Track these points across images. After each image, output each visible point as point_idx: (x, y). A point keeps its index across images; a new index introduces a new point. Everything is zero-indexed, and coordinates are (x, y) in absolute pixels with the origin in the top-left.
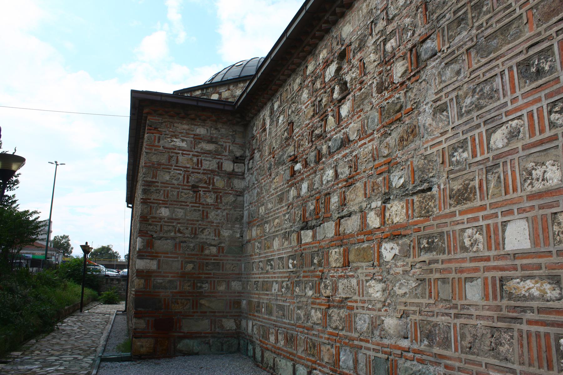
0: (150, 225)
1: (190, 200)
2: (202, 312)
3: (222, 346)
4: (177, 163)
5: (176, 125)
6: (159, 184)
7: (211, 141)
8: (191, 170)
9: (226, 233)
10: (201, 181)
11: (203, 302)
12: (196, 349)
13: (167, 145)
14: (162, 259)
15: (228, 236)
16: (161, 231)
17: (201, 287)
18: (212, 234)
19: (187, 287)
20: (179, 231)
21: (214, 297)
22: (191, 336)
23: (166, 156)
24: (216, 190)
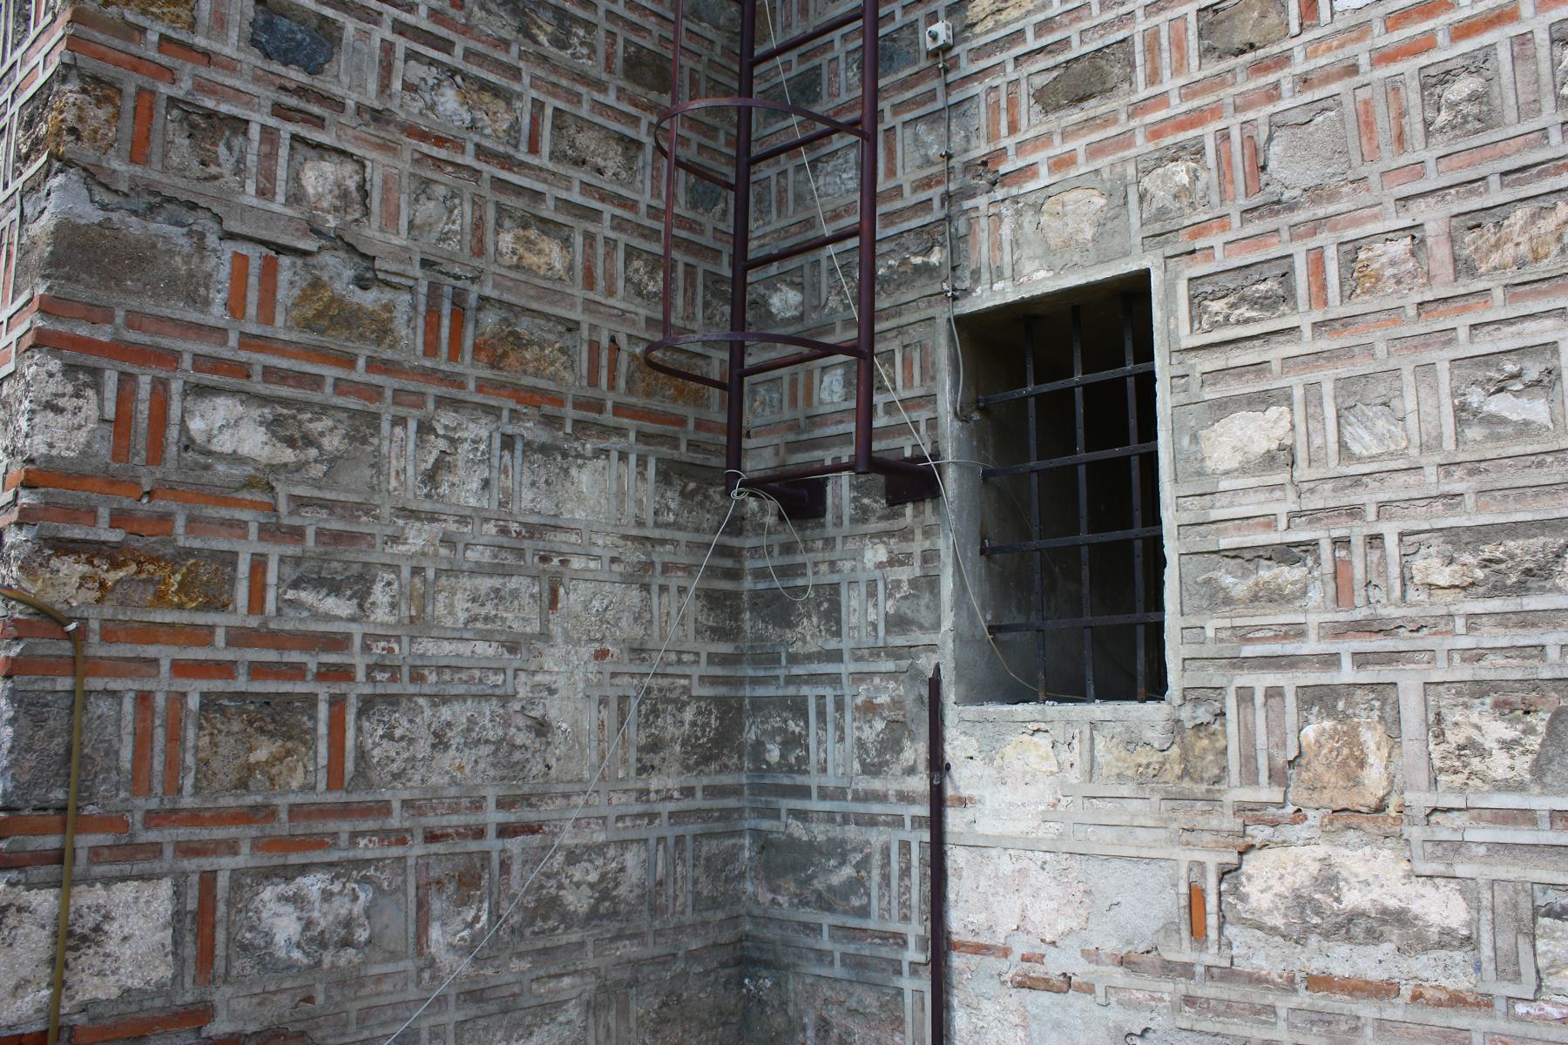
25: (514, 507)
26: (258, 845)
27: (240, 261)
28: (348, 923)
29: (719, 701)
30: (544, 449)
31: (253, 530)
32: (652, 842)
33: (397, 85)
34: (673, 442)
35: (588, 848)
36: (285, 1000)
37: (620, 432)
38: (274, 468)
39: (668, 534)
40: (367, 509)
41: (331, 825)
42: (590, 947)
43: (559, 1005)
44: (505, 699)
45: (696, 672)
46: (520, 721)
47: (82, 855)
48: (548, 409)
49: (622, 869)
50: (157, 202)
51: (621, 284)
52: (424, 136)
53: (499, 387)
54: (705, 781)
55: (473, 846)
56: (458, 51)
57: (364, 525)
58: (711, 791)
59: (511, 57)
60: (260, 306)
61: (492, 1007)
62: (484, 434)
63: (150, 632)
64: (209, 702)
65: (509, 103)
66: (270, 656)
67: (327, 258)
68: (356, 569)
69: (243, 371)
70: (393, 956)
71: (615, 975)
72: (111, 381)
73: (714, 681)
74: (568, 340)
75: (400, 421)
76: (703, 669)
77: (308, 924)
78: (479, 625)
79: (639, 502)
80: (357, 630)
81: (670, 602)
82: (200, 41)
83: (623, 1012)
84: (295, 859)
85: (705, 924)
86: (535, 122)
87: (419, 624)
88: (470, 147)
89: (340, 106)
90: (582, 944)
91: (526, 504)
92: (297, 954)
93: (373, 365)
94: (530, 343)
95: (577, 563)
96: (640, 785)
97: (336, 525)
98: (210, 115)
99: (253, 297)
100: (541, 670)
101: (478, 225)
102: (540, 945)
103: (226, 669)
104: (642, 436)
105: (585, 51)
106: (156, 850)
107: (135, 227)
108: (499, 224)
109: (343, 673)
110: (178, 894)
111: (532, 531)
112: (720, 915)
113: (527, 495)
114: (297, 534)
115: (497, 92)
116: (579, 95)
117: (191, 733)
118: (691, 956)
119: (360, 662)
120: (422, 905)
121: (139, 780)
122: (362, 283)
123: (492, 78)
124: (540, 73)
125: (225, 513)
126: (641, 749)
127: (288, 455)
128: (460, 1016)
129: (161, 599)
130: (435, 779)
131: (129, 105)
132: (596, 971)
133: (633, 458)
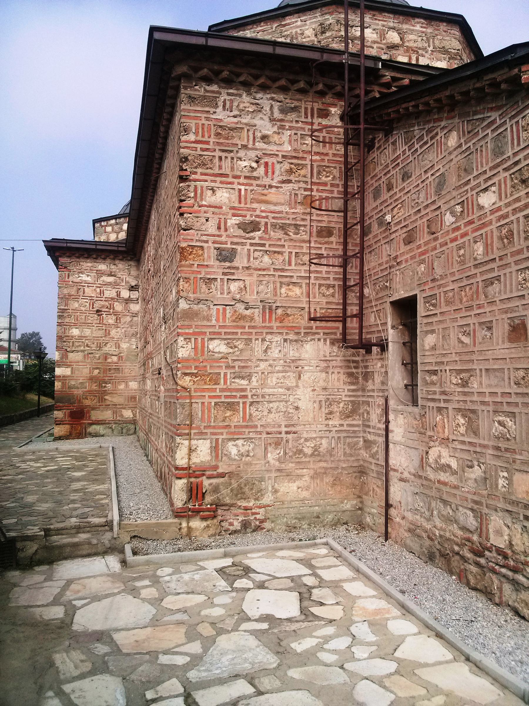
0: (65, 342)
1: (95, 322)
2: (106, 405)
3: (122, 429)
4: (84, 293)
5: (81, 263)
6: (70, 311)
7: (110, 275)
9: (124, 346)
10: (103, 306)
11: (106, 397)
12: (102, 432)
13: (75, 280)
14: (75, 366)
15: (127, 348)
16: (73, 346)
17: (105, 387)
18: (114, 347)
19: (94, 387)
20: (87, 346)
22: (98, 423)
23: (75, 288)
24: (116, 314)
25: (288, 356)
27: (218, 310)
28: (248, 451)
29: (352, 402)
30: (296, 341)
31: (224, 367)
32: (330, 438)
33: (252, 259)
34: (335, 334)
35: (311, 438)
36: (234, 467)
37: (318, 333)
40: (250, 360)
41: (244, 430)
42: (312, 463)
43: (303, 476)
44: (286, 402)
45: (344, 394)
46: (291, 407)
47: (192, 434)
48: (296, 331)
50: (199, 301)
52: (260, 270)
53: (283, 327)
54: (347, 423)
55: (279, 436)
56: (267, 246)
57: (250, 364)
58: (349, 425)
59: (282, 243)
61: (284, 474)
62: (279, 339)
63: (203, 390)
64: (216, 404)
65: (282, 254)
66: (229, 394)
67: (237, 305)
68: (248, 374)
69: (220, 333)
70: (259, 459)
71: (319, 471)
72: (193, 340)
73: (350, 396)
74: (302, 312)
75: (257, 339)
76: (346, 393)
77: (239, 451)
78: (280, 385)
79: (325, 351)
80: (248, 387)
82: (206, 263)
83: (322, 480)
85: (348, 460)
86: (290, 258)
87: (263, 385)
88: (272, 269)
89: (237, 268)
90: (309, 462)
92: (236, 457)
93: (249, 327)
94: (291, 315)
95: (306, 368)
96: (326, 423)
97: (242, 365)
98: (209, 279)
99: (221, 318)
101: (275, 289)
103: (219, 397)
104: (324, 333)
105: (304, 233)
107: (195, 307)
108: (281, 287)
109: (246, 397)
111: (293, 361)
112: (353, 459)
113: (291, 352)
114: (234, 367)
115: (279, 253)
117: (213, 410)
119: (250, 395)
120: (266, 449)
121: (202, 420)
122: (246, 309)
124: (291, 244)
127: (231, 350)
129: (205, 383)
130: (269, 420)
132: (313, 469)
133: (322, 340)
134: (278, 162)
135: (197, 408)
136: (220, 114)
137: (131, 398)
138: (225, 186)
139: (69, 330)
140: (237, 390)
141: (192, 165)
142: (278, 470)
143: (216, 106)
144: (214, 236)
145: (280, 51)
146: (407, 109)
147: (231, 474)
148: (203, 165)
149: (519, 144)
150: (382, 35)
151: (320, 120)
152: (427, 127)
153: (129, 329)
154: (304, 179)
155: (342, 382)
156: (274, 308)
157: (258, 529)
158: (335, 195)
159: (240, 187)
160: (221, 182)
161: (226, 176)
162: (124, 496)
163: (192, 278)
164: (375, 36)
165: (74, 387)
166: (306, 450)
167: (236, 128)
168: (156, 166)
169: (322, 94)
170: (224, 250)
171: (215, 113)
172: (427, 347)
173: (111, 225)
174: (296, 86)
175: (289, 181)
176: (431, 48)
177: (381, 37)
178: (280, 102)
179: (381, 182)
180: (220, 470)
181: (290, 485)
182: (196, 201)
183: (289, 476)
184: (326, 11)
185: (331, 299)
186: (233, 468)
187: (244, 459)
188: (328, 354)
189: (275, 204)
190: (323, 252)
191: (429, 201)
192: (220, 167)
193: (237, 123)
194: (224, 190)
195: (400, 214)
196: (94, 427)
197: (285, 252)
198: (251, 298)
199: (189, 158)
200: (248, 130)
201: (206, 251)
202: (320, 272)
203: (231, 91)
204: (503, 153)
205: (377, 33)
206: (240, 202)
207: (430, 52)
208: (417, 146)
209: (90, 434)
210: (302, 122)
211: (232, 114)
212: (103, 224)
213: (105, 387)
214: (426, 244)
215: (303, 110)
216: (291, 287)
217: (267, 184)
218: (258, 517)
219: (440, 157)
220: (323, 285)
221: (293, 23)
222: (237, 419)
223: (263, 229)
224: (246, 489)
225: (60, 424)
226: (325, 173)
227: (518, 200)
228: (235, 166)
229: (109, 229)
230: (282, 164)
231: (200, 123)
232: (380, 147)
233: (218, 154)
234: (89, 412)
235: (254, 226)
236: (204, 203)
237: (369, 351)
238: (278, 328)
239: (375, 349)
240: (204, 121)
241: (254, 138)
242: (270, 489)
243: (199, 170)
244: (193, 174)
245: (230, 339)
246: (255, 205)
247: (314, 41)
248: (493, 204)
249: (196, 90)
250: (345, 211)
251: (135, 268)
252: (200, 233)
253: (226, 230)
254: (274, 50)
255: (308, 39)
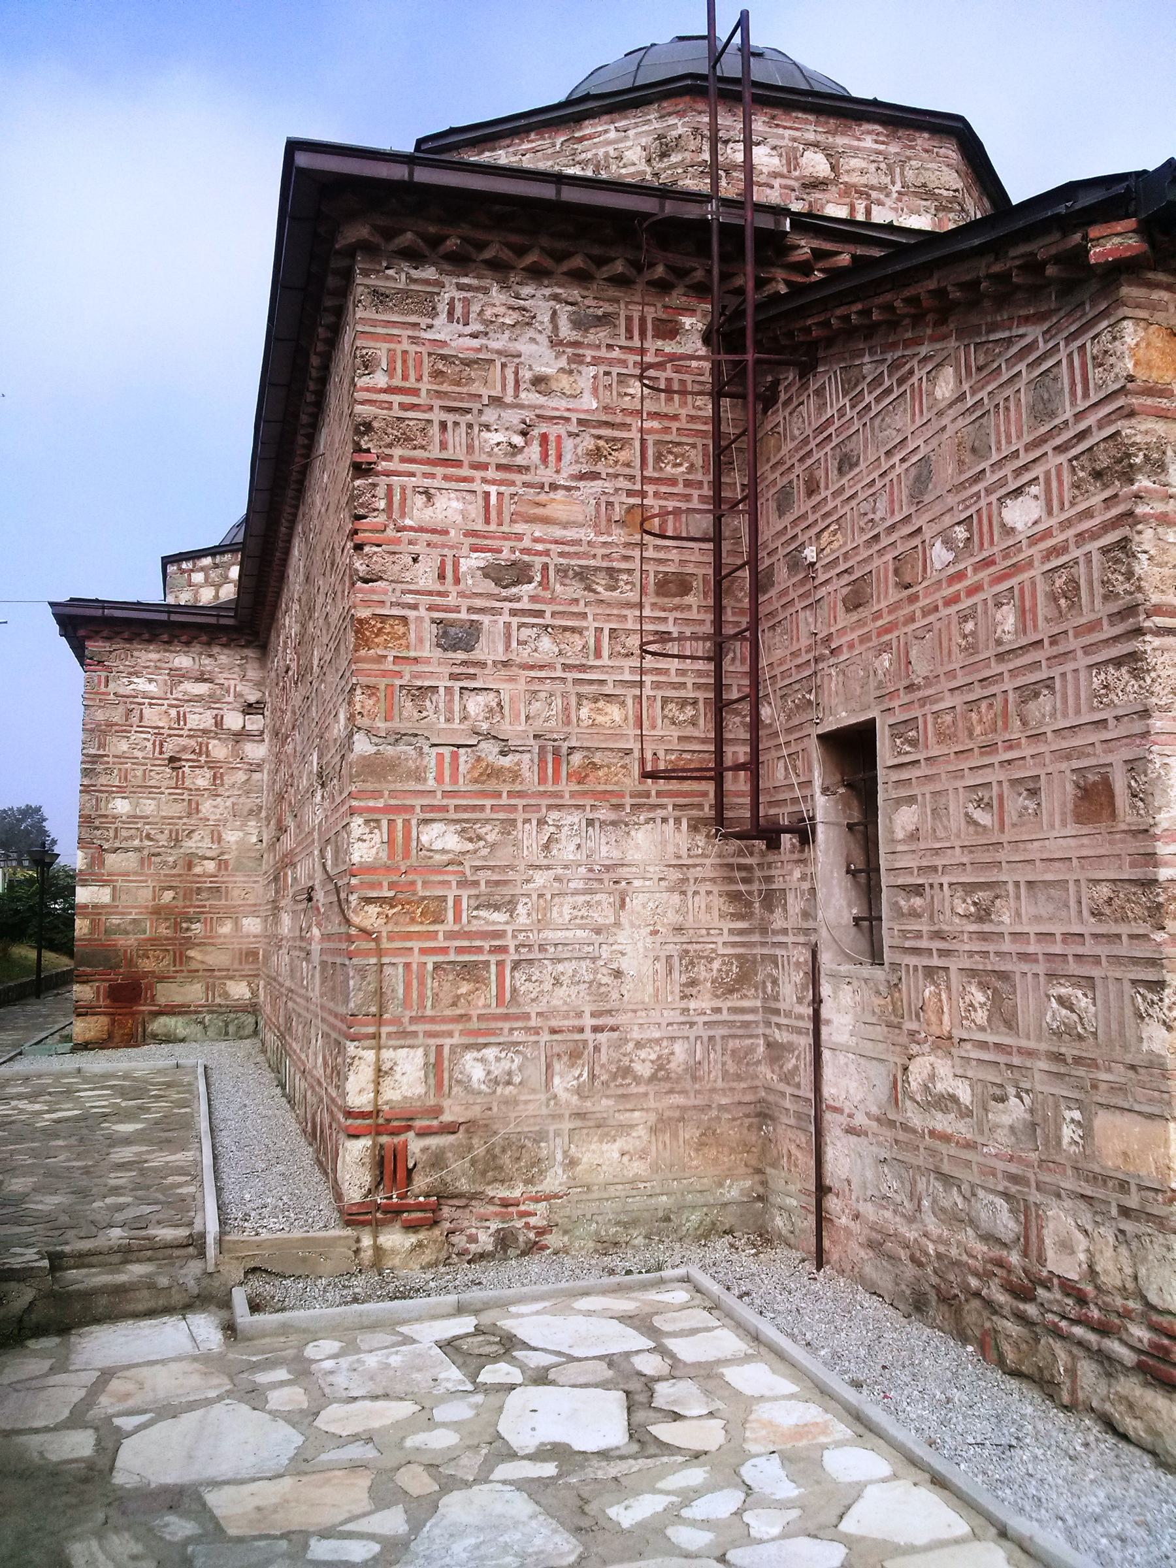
0: (97, 828)
1: (166, 783)
3: (227, 1026)
5: (136, 654)
6: (110, 759)
7: (201, 679)
8: (166, 731)
9: (231, 837)
10: (184, 749)
11: (191, 953)
12: (181, 1032)
13: (121, 691)
14: (118, 884)
15: (237, 842)
16: (116, 837)
17: (188, 929)
18: (208, 840)
19: (164, 930)
20: (148, 837)
21: (213, 944)
23: (121, 709)
24: (213, 765)
26: (462, 1033)
27: (440, 756)
28: (510, 1073)
29: (738, 957)
30: (614, 823)
31: (454, 884)
32: (692, 1039)
33: (514, 644)
34: (700, 806)
35: (650, 1041)
36: (478, 1109)
37: (663, 806)
38: (463, 853)
39: (698, 861)
40: (512, 867)
41: (500, 1024)
42: (651, 1096)
43: (632, 1126)
44: (594, 960)
45: (720, 940)
46: (605, 971)
47: (384, 1036)
48: (614, 801)
49: (672, 1053)
50: (399, 737)
51: (659, 721)
52: (532, 667)
53: (584, 794)
54: (730, 1004)
55: (577, 1037)
56: (548, 615)
57: (511, 875)
58: (733, 1010)
59: (580, 608)
60: (451, 776)
61: (591, 1123)
62: (576, 820)
63: (409, 936)
64: (437, 966)
65: (581, 633)
66: (466, 943)
67: (483, 745)
68: (508, 898)
69: (444, 808)
70: (534, 1091)
71: (667, 1114)
72: (384, 823)
74: (627, 760)
75: (528, 821)
76: (726, 937)
77: (489, 1073)
78: (578, 921)
80: (509, 928)
81: (701, 901)
82: (412, 654)
83: (675, 1136)
84: (481, 1040)
85: (732, 1089)
86: (598, 641)
87: (542, 924)
88: (559, 667)
89: (482, 665)
90: (646, 1094)
91: (604, 854)
92: (483, 1087)
93: (510, 794)
94: (602, 766)
95: (636, 883)
97: (496, 877)
98: (420, 688)
99: (447, 773)
100: (616, 942)
101: (566, 709)
102: (620, 1091)
103: (444, 950)
104: (675, 806)
105: (628, 587)
106: (414, 1034)
107: (390, 751)
108: (579, 704)
109: (503, 949)
110: (426, 1055)
111: (608, 868)
112: (743, 1085)
113: (604, 849)
114: (476, 883)
115: (573, 630)
116: (625, 616)
117: (429, 981)
118: (721, 1107)
119: (511, 944)
121: (406, 1003)
122: (503, 753)
123: (569, 623)
124: (599, 611)
125: (440, 878)
126: (684, 985)
127: (470, 846)
128: (572, 1126)
129: (413, 920)
130: (555, 1002)
131: (382, 695)
132: (656, 1110)
133: (671, 821)
134: (570, 434)
135: (395, 977)
136: (443, 330)
137: (247, 955)
138: (454, 485)
139: (108, 802)
140: (484, 935)
141: (381, 439)
142: (580, 1115)
143: (433, 313)
144: (430, 593)
145: (570, 195)
146: (846, 318)
147: (471, 1126)
148: (406, 439)
149: (1086, 395)
150: (792, 160)
151: (660, 343)
152: (889, 357)
153: (243, 799)
154: (627, 471)
155: (716, 914)
156: (564, 751)
157: (533, 1248)
158: (695, 504)
159: (487, 488)
160: (446, 478)
161: (457, 463)
162: (230, 1177)
163: (382, 687)
164: (776, 161)
165: (118, 930)
166: (638, 1067)
167: (477, 361)
168: (301, 440)
169: (663, 287)
170: (452, 623)
171: (430, 327)
172: (900, 835)
173: (202, 569)
174: (606, 271)
175: (595, 476)
176: (898, 187)
177: (789, 164)
178: (572, 304)
179: (793, 476)
180: (447, 1118)
181: (605, 1147)
182: (389, 518)
183: (603, 1128)
184: (671, 109)
185: (689, 731)
186: (475, 1112)
187: (499, 1090)
188: (684, 852)
189: (565, 525)
190: (670, 627)
191: (898, 517)
192: (443, 446)
193: (479, 350)
194: (452, 495)
195: (835, 545)
196: (163, 1020)
197: (587, 628)
198: (513, 728)
199: (375, 424)
200: (504, 366)
201: (412, 626)
202: (666, 672)
203: (465, 280)
204: (1052, 415)
205: (780, 155)
206: (487, 521)
207: (895, 195)
208: (868, 398)
209: (154, 1036)
210: (621, 347)
211: (468, 330)
212: (184, 566)
213: (188, 929)
214: (892, 608)
215: (622, 322)
216: (601, 704)
217: (547, 481)
218: (533, 1221)
219: (918, 423)
220: (672, 700)
221: (600, 134)
222: (484, 1001)
223: (538, 578)
224: (506, 1160)
225: (86, 1014)
226: (671, 457)
227: (1088, 514)
228: (476, 443)
229: (198, 577)
230: (578, 439)
231: (399, 348)
232: (789, 400)
233: (437, 416)
234: (151, 987)
235: (518, 573)
236: (408, 522)
237: (774, 845)
238: (573, 794)
239: (786, 838)
240: (406, 345)
241: (517, 382)
242: (559, 1157)
243: (397, 452)
244: (384, 459)
245: (467, 821)
246: (519, 528)
247: (645, 173)
248: (1035, 523)
249: (388, 278)
250: (717, 538)
251: (256, 665)
252: (399, 587)
253: (457, 581)
254: (558, 192)
255: (632, 169)
